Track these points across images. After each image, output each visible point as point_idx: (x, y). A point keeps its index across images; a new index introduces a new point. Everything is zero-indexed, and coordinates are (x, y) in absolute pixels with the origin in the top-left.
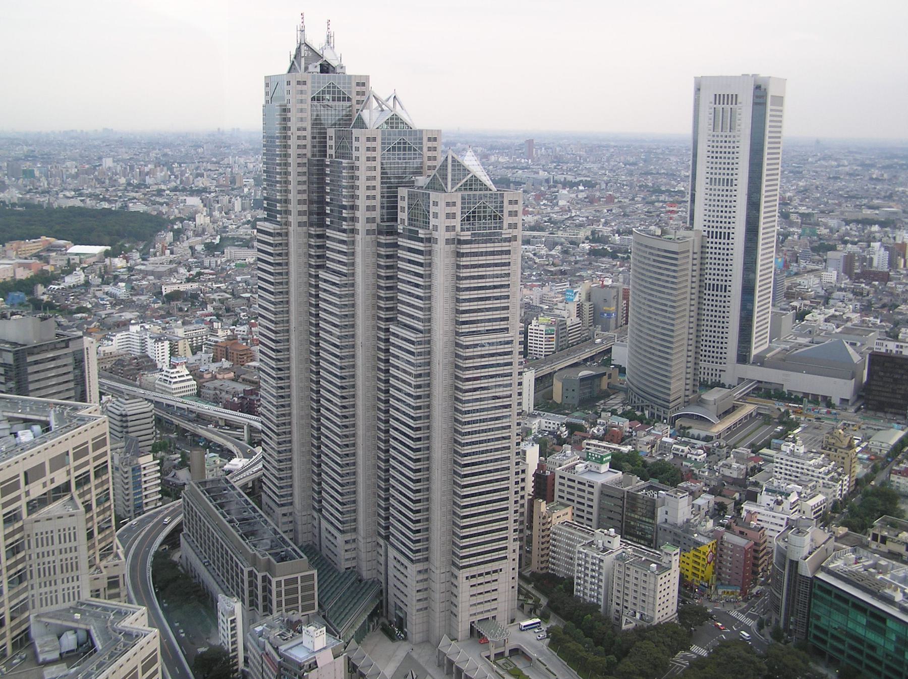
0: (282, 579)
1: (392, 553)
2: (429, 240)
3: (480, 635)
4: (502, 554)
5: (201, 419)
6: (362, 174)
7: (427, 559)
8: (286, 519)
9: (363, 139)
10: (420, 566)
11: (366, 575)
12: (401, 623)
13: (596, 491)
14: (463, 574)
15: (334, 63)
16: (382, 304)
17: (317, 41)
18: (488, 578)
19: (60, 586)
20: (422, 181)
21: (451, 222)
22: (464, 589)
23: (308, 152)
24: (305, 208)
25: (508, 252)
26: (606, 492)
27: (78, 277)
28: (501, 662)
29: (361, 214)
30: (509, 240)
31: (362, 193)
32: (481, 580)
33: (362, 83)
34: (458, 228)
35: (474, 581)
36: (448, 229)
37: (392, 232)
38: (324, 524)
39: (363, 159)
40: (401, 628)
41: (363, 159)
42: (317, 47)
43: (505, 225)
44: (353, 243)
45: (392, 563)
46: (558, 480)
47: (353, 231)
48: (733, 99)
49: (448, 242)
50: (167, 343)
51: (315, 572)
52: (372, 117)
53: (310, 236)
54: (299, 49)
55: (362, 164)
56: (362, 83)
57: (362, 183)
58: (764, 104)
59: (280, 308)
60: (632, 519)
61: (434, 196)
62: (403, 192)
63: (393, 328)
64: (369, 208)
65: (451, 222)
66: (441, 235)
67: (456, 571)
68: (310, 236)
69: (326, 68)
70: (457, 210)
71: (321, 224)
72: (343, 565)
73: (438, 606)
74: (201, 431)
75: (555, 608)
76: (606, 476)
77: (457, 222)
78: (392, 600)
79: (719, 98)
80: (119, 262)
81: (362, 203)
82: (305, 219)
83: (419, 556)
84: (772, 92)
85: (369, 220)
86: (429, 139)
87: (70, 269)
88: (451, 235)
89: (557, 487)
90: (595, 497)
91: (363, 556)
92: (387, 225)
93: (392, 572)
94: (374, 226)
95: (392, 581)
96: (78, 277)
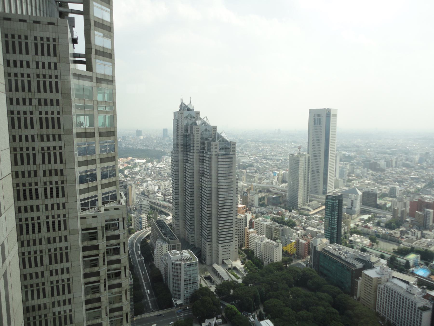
0: (172, 245)
1: (203, 240)
2: (211, 155)
3: (225, 263)
4: (231, 240)
5: (164, 207)
6: (195, 137)
7: (211, 241)
8: (177, 231)
9: (195, 128)
10: (209, 243)
11: (197, 246)
12: (205, 259)
13: (265, 226)
14: (220, 245)
15: (191, 108)
16: (200, 172)
17: (187, 103)
18: (227, 247)
19: (41, 179)
20: (211, 139)
21: (216, 150)
22: (220, 249)
23: (183, 132)
24: (183, 146)
25: (232, 158)
26: (268, 227)
27: (138, 169)
28: (230, 271)
29: (195, 148)
30: (231, 155)
31: (195, 142)
32: (225, 247)
33: (198, 113)
34: (218, 152)
35: (223, 248)
36: (215, 152)
37: (203, 152)
38: (203, 240)
39: (195, 133)
40: (205, 261)
41: (195, 133)
42: (187, 104)
43: (231, 150)
44: (193, 156)
45: (203, 242)
46: (255, 223)
47: (211, 155)
48: (320, 115)
49: (215, 155)
50: (158, 186)
51: (181, 243)
52: (199, 122)
53: (184, 154)
54: (181, 105)
55: (195, 135)
56: (198, 113)
57: (195, 140)
58: (330, 117)
59: (191, 177)
60: (271, 234)
61: (212, 143)
62: (206, 142)
63: (203, 178)
64: (197, 146)
65: (216, 150)
66: (214, 153)
67: (218, 244)
68: (184, 154)
69: (188, 110)
70: (218, 147)
71: (187, 151)
72: (191, 243)
73: (214, 255)
74: (163, 210)
75: (249, 257)
76: (269, 222)
77: (218, 150)
78: (203, 253)
79: (316, 115)
80: (150, 165)
81: (195, 145)
82: (182, 149)
83: (208, 240)
84: (332, 113)
85: (197, 150)
86: (214, 128)
87: (135, 165)
88: (216, 153)
89: (255, 225)
90: (265, 228)
91: (196, 241)
92: (202, 151)
93: (203, 245)
94: (199, 151)
95: (203, 248)
96: (138, 169)
